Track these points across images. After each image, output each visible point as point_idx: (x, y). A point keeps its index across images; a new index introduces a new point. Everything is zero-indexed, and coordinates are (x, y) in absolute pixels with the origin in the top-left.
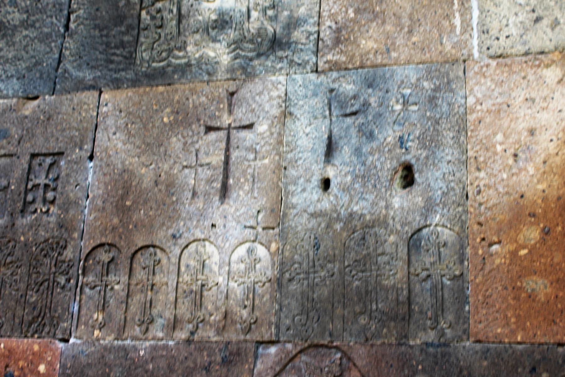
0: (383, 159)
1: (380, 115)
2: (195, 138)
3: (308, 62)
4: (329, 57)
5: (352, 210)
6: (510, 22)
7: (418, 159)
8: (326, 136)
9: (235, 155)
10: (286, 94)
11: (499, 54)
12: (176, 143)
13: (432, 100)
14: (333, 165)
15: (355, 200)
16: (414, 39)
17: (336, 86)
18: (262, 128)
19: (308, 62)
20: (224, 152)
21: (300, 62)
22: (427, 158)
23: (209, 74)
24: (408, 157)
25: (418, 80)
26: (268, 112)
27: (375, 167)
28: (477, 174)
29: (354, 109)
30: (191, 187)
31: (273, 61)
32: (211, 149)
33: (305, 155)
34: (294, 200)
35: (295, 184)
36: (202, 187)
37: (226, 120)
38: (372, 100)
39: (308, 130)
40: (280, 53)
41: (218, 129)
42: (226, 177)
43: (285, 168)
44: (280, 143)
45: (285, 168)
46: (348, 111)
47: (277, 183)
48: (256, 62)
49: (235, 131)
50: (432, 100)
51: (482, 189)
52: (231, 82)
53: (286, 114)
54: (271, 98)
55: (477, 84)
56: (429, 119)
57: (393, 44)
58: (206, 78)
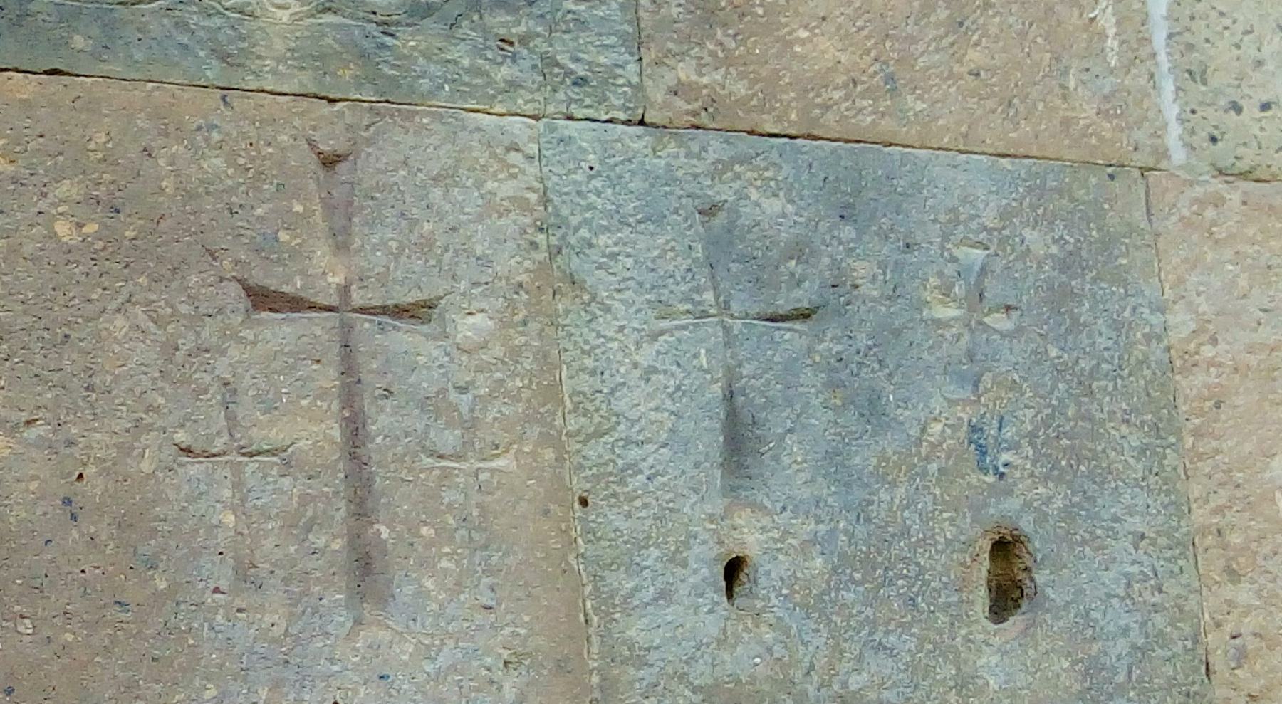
0: (926, 503)
1: (897, 333)
2: (209, 332)
3: (609, 76)
4: (685, 71)
5: (845, 685)
6: (1267, 50)
7: (1042, 518)
8: (717, 390)
9: (382, 421)
10: (545, 201)
11: (1243, 166)
12: (126, 341)
13: (1060, 298)
14: (757, 507)
15: (852, 649)
16: (975, 56)
17: (724, 192)
18: (472, 325)
19: (609, 76)
20: (335, 406)
21: (581, 71)
22: (1068, 513)
23: (224, 58)
24: (1011, 505)
25: (1005, 215)
26: (485, 262)
27: (905, 532)
28: (1228, 591)
29: (802, 297)
30: (221, 539)
31: (478, 52)
32: (281, 384)
33: (653, 456)
34: (636, 630)
35: (634, 568)
36: (272, 546)
37: (325, 272)
38: (862, 269)
39: (646, 356)
40: (499, 21)
41: (297, 304)
42: (362, 506)
43: (584, 502)
44: (552, 392)
45: (584, 502)
46: (783, 304)
47: (564, 558)
48: (407, 41)
49: (365, 324)
50: (1060, 298)
51: (1252, 644)
52: (325, 109)
53: (555, 281)
54: (491, 208)
55: (1193, 264)
56: (1060, 371)
57: (906, 60)
58: (213, 72)
